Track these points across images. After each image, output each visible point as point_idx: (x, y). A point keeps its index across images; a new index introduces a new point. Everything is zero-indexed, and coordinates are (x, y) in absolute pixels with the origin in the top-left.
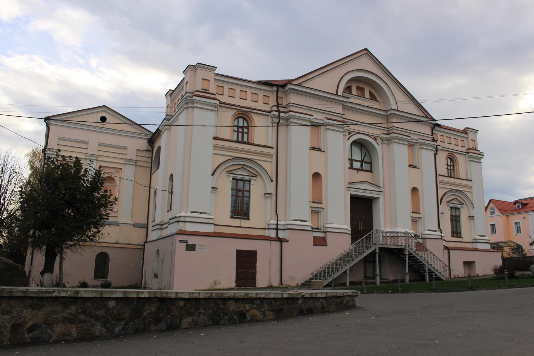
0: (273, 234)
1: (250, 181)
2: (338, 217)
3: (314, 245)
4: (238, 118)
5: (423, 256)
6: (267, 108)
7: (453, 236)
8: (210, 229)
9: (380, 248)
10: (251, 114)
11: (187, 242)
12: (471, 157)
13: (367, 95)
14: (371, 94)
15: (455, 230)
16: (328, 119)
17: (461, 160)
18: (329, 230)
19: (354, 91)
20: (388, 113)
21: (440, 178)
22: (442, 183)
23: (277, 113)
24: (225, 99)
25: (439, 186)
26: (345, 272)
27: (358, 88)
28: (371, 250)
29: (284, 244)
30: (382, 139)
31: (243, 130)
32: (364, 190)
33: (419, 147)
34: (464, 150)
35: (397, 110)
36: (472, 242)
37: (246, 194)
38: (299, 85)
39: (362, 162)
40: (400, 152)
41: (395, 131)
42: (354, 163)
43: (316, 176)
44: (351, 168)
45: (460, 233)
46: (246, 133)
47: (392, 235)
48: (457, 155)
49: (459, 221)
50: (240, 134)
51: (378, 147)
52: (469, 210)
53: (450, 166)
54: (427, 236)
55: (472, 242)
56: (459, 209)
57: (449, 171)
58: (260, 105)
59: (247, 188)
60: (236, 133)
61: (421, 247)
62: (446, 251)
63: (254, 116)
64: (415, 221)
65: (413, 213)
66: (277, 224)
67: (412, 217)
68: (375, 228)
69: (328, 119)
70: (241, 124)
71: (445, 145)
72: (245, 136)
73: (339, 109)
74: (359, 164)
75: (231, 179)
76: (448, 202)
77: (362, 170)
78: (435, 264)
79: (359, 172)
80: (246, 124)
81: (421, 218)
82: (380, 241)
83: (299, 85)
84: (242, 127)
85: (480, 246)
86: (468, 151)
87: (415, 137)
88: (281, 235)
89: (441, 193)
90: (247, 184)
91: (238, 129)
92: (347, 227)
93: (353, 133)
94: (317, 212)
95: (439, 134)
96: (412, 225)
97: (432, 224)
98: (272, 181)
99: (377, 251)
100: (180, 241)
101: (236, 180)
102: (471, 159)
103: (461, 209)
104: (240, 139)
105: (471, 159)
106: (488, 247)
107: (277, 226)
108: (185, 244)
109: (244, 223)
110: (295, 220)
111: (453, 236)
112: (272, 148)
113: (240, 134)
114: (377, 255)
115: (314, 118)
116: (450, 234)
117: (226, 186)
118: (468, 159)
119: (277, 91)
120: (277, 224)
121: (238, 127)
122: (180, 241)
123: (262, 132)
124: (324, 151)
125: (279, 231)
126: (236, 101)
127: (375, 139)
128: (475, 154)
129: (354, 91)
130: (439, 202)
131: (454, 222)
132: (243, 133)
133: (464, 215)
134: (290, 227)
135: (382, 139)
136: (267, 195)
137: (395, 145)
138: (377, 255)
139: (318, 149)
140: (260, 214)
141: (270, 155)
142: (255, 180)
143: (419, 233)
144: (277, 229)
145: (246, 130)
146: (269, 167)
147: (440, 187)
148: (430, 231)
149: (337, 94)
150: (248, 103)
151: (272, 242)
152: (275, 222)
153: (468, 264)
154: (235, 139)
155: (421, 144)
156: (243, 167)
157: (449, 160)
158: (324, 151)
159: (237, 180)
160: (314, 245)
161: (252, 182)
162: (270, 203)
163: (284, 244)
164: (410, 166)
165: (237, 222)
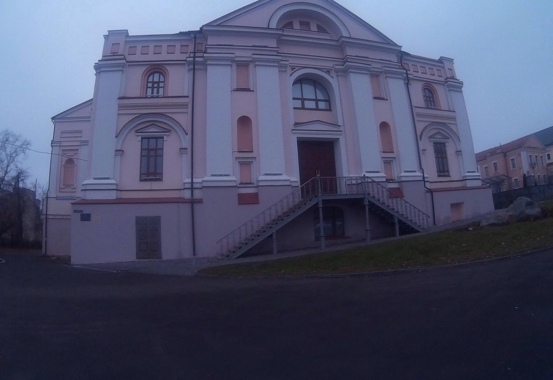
0: (187, 195)
1: (163, 138)
2: (278, 166)
3: (239, 204)
4: (153, 73)
5: (391, 204)
6: (183, 57)
7: (439, 176)
14: (319, 27)
15: (441, 169)
17: (440, 91)
19: (297, 25)
20: (340, 42)
21: (416, 110)
22: (419, 115)
23: (192, 59)
24: (138, 57)
25: (416, 119)
26: (271, 236)
27: (302, 23)
28: (313, 203)
29: (196, 206)
30: (337, 71)
31: (158, 85)
32: (318, 132)
33: (384, 76)
34: (442, 79)
35: (350, 38)
36: (462, 181)
37: (159, 152)
38: (219, 25)
39: (317, 101)
40: (361, 84)
42: (306, 102)
44: (303, 108)
45: (448, 171)
46: (161, 87)
47: (359, 181)
49: (446, 158)
50: (155, 90)
51: (334, 81)
52: (455, 144)
53: (429, 97)
54: (403, 179)
55: (462, 181)
56: (444, 144)
57: (429, 103)
58: (178, 56)
59: (159, 146)
60: (149, 90)
61: (397, 193)
62: (429, 195)
63: (167, 67)
64: (388, 162)
65: (384, 152)
66: (192, 183)
67: (382, 158)
68: (338, 174)
69: (254, 54)
70: (156, 79)
71: (420, 75)
72: (161, 90)
73: (273, 43)
75: (140, 139)
76: (431, 137)
77: (317, 109)
78: (408, 213)
80: (162, 79)
81: (395, 158)
82: (343, 190)
83: (219, 25)
84: (158, 83)
85: (469, 184)
86: (446, 81)
87: (379, 66)
88: (198, 194)
89: (420, 127)
91: (153, 85)
92: (295, 178)
93: (297, 68)
94: (249, 164)
95: (410, 64)
97: (411, 163)
98: (187, 134)
99: (320, 205)
103: (447, 144)
106: (479, 183)
107: (192, 185)
109: (155, 185)
110: (213, 175)
111: (439, 176)
112: (188, 97)
113: (155, 90)
114: (321, 210)
115: (236, 57)
116: (436, 174)
117: (134, 146)
118: (447, 89)
119: (195, 38)
120: (192, 183)
121: (153, 83)
123: (178, 81)
124: (253, 91)
125: (195, 191)
126: (151, 57)
127: (328, 72)
128: (454, 85)
129: (297, 25)
130: (418, 138)
131: (440, 160)
132: (158, 88)
133: (450, 150)
134: (205, 184)
135: (337, 71)
136: (182, 150)
137: (351, 75)
138: (321, 210)
139: (248, 90)
140: (175, 174)
141: (185, 106)
142: (168, 136)
143: (395, 176)
144: (192, 189)
145: (161, 85)
146: (184, 119)
147: (418, 121)
148: (408, 172)
149: (268, 28)
150: (164, 56)
151: (180, 204)
152: (189, 180)
153: (456, 206)
155: (387, 72)
156: (153, 124)
157: (427, 91)
158: (253, 91)
159: (149, 138)
160: (239, 204)
161: (165, 138)
162: (186, 159)
163: (196, 206)
164: (375, 98)
165: (147, 185)
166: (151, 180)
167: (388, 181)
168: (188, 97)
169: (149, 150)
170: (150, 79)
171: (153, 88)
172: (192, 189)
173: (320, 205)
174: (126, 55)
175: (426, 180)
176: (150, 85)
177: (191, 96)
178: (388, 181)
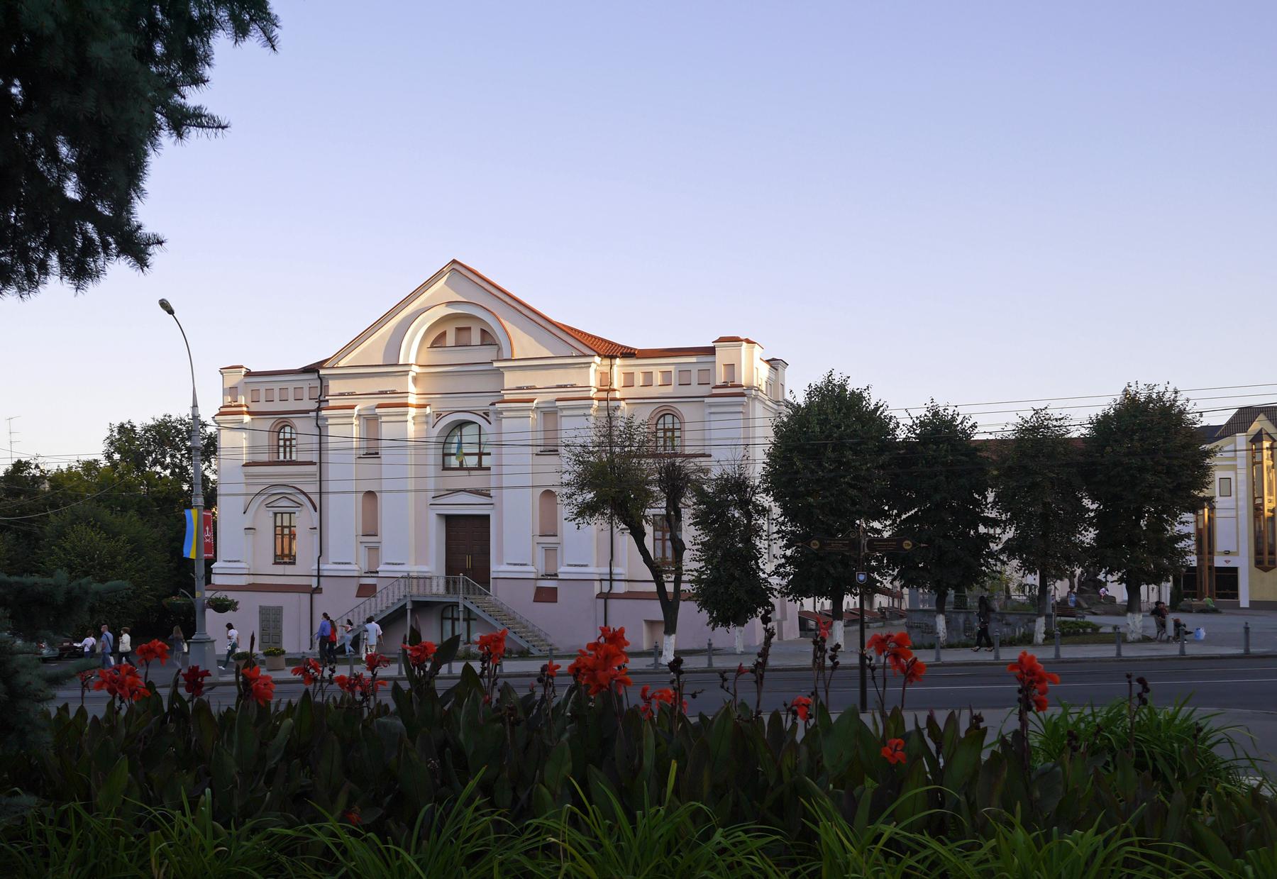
4: (284, 427)
8: (243, 581)
9: (414, 602)
10: (294, 421)
12: (711, 405)
13: (476, 337)
14: (483, 331)
16: (380, 406)
18: (380, 574)
19: (450, 339)
41: (506, 397)
43: (371, 494)
48: (678, 406)
60: (282, 450)
63: (294, 421)
70: (288, 436)
75: (271, 514)
79: (473, 473)
90: (286, 517)
94: (377, 548)
96: (546, 557)
99: (409, 606)
101: (275, 514)
102: (713, 410)
105: (713, 410)
109: (289, 569)
112: (315, 464)
121: (285, 440)
127: (486, 415)
144: (319, 576)
145: (294, 442)
150: (291, 405)
154: (282, 458)
156: (284, 496)
163: (316, 596)
165: (280, 569)
166: (285, 563)
167: (547, 576)
168: (315, 464)
169: (283, 527)
170: (281, 436)
171: (285, 446)
172: (319, 576)
174: (249, 404)
175: (615, 577)
176: (282, 443)
178: (547, 576)
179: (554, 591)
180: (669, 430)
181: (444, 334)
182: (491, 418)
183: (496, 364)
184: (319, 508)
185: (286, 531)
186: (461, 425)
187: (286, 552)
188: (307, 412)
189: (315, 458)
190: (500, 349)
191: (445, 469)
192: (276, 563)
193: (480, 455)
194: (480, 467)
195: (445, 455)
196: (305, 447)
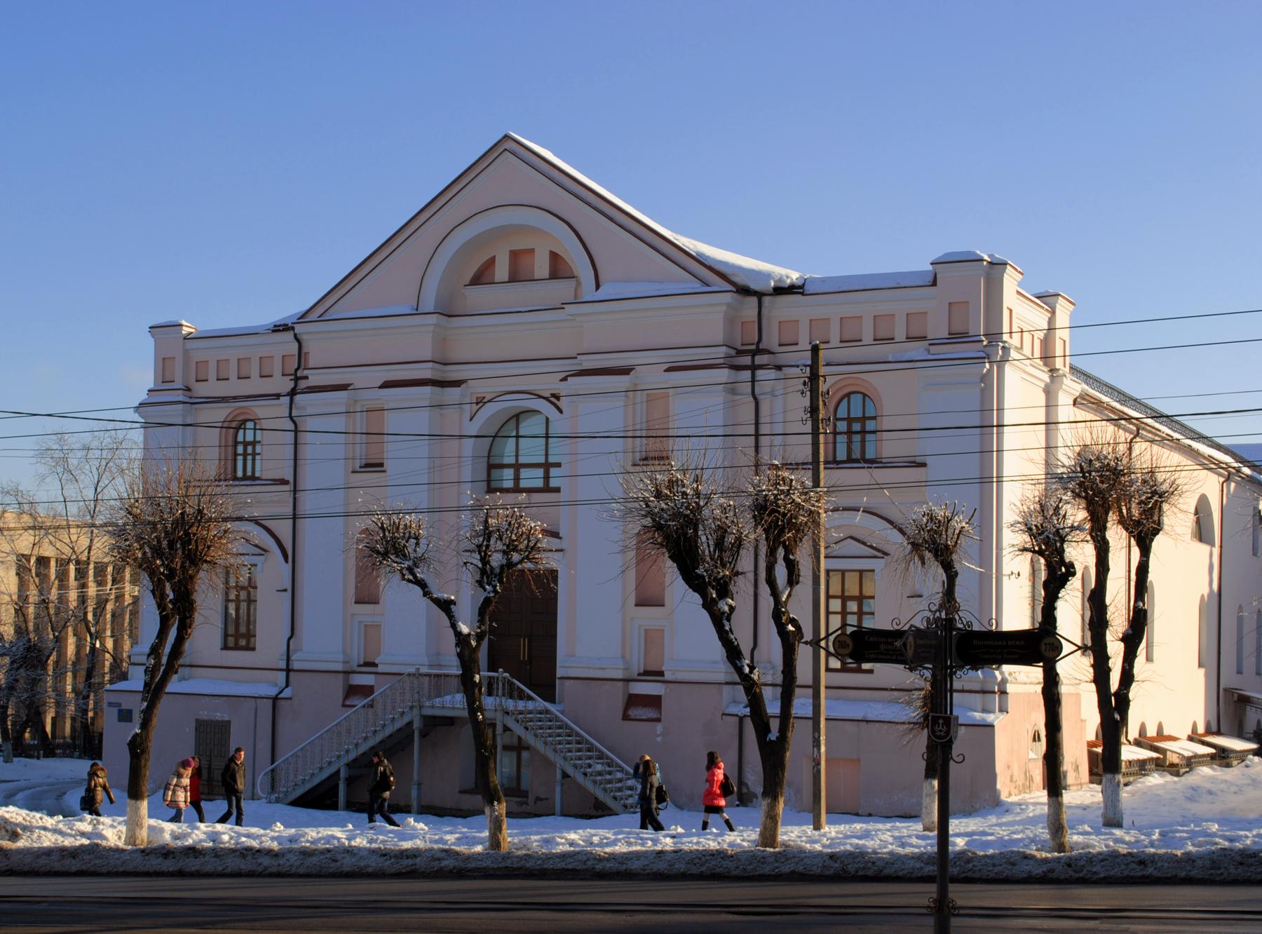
11: (119, 705)
18: (380, 669)
50: (250, 458)
70: (250, 438)
74: (540, 472)
91: (245, 449)
98: (286, 561)
99: (416, 725)
100: (110, 704)
104: (249, 473)
108: (115, 710)
112: (287, 483)
113: (250, 458)
121: (246, 444)
122: (110, 704)
132: (254, 454)
144: (288, 670)
150: (256, 385)
168: (287, 483)
171: (245, 455)
173: (416, 725)
176: (240, 449)
177: (291, 480)
179: (654, 702)
180: (856, 420)
181: (491, 262)
182: (563, 403)
183: (570, 309)
184: (290, 555)
185: (243, 595)
186: (517, 417)
187: (243, 629)
188: (278, 396)
189: (289, 476)
190: (579, 284)
191: (490, 490)
192: (225, 647)
193: (547, 466)
194: (547, 489)
195: (491, 467)
196: (273, 458)
